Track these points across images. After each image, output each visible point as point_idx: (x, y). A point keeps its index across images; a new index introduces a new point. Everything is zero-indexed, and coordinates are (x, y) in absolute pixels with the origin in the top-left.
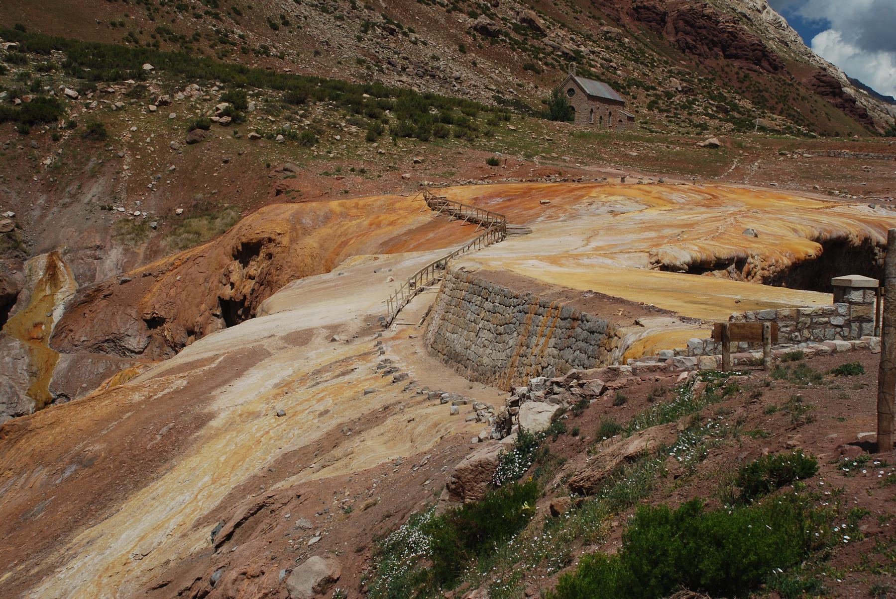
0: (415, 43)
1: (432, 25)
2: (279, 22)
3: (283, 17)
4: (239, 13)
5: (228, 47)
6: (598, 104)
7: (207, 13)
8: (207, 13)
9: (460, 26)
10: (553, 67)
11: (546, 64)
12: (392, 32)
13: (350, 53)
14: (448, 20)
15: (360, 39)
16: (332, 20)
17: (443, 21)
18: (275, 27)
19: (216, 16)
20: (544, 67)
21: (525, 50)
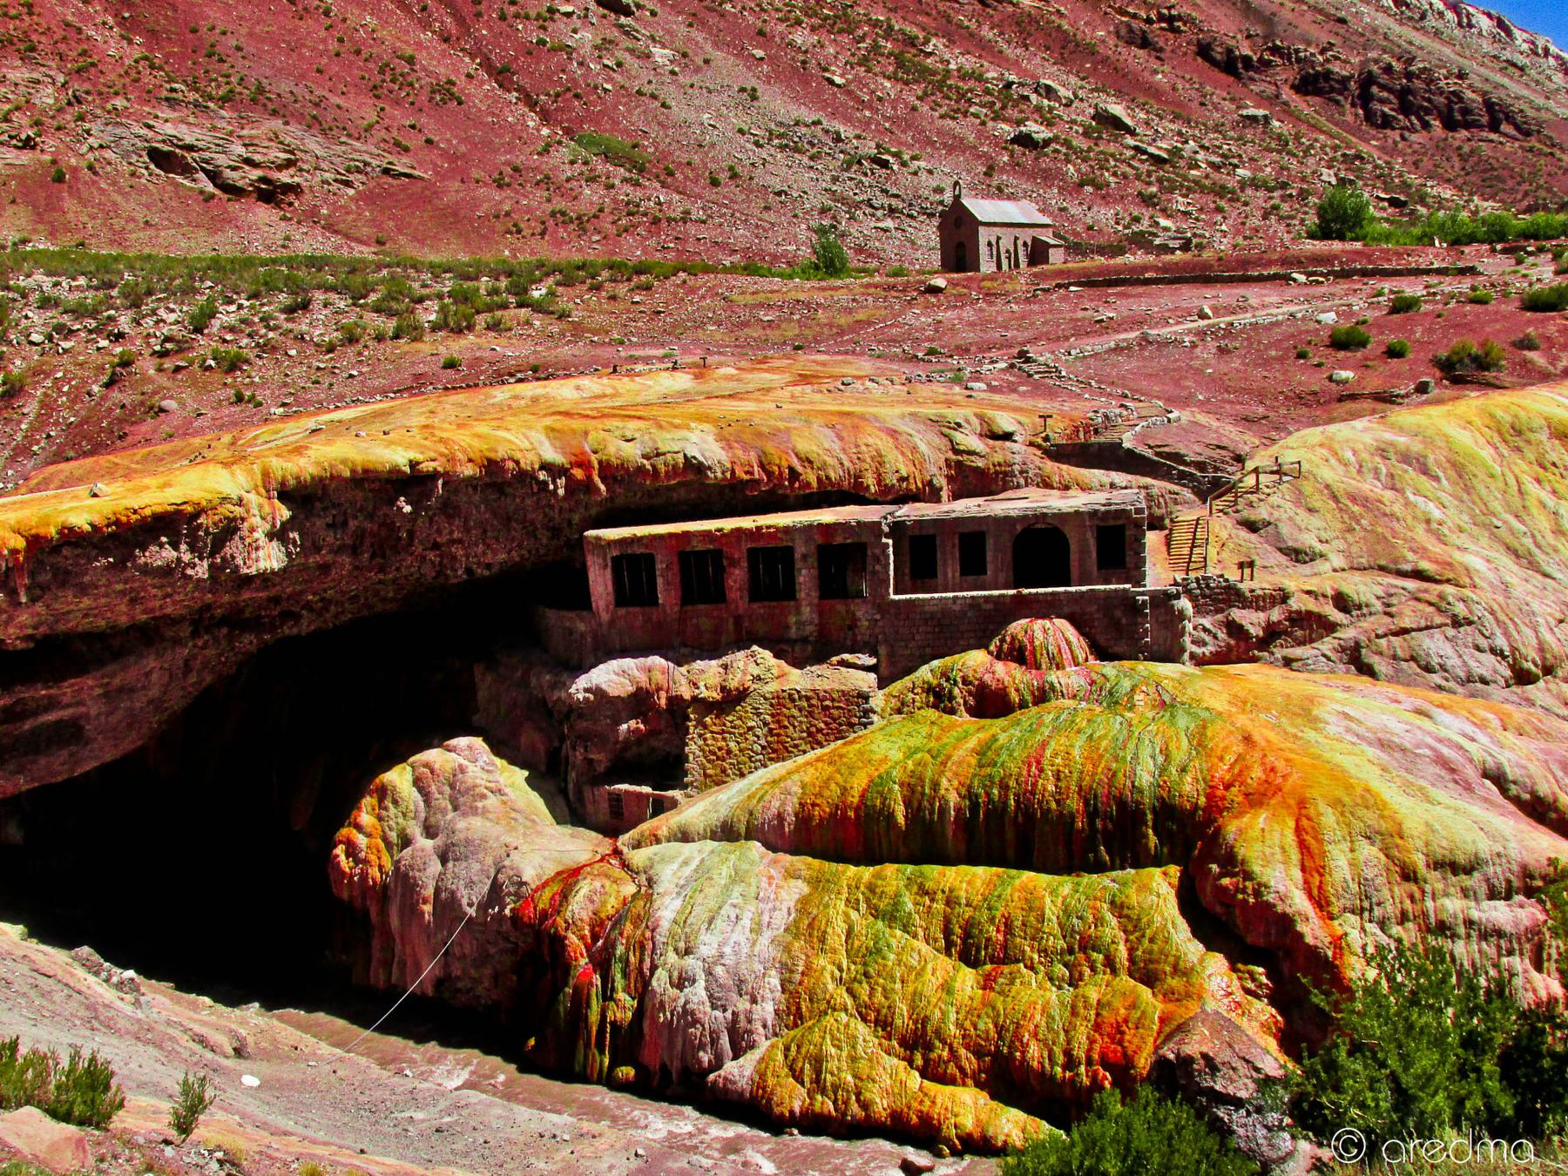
0: (915, 173)
1: (956, 146)
2: (723, 177)
3: (731, 169)
4: (671, 174)
5: (635, 220)
6: (998, 231)
7: (625, 180)
8: (625, 180)
9: (996, 141)
10: (1125, 176)
11: (1115, 174)
12: (884, 164)
13: (816, 200)
14: (979, 135)
15: (835, 180)
16: (805, 160)
17: (971, 138)
18: (715, 183)
19: (637, 184)
20: (1111, 179)
21: (1085, 160)
